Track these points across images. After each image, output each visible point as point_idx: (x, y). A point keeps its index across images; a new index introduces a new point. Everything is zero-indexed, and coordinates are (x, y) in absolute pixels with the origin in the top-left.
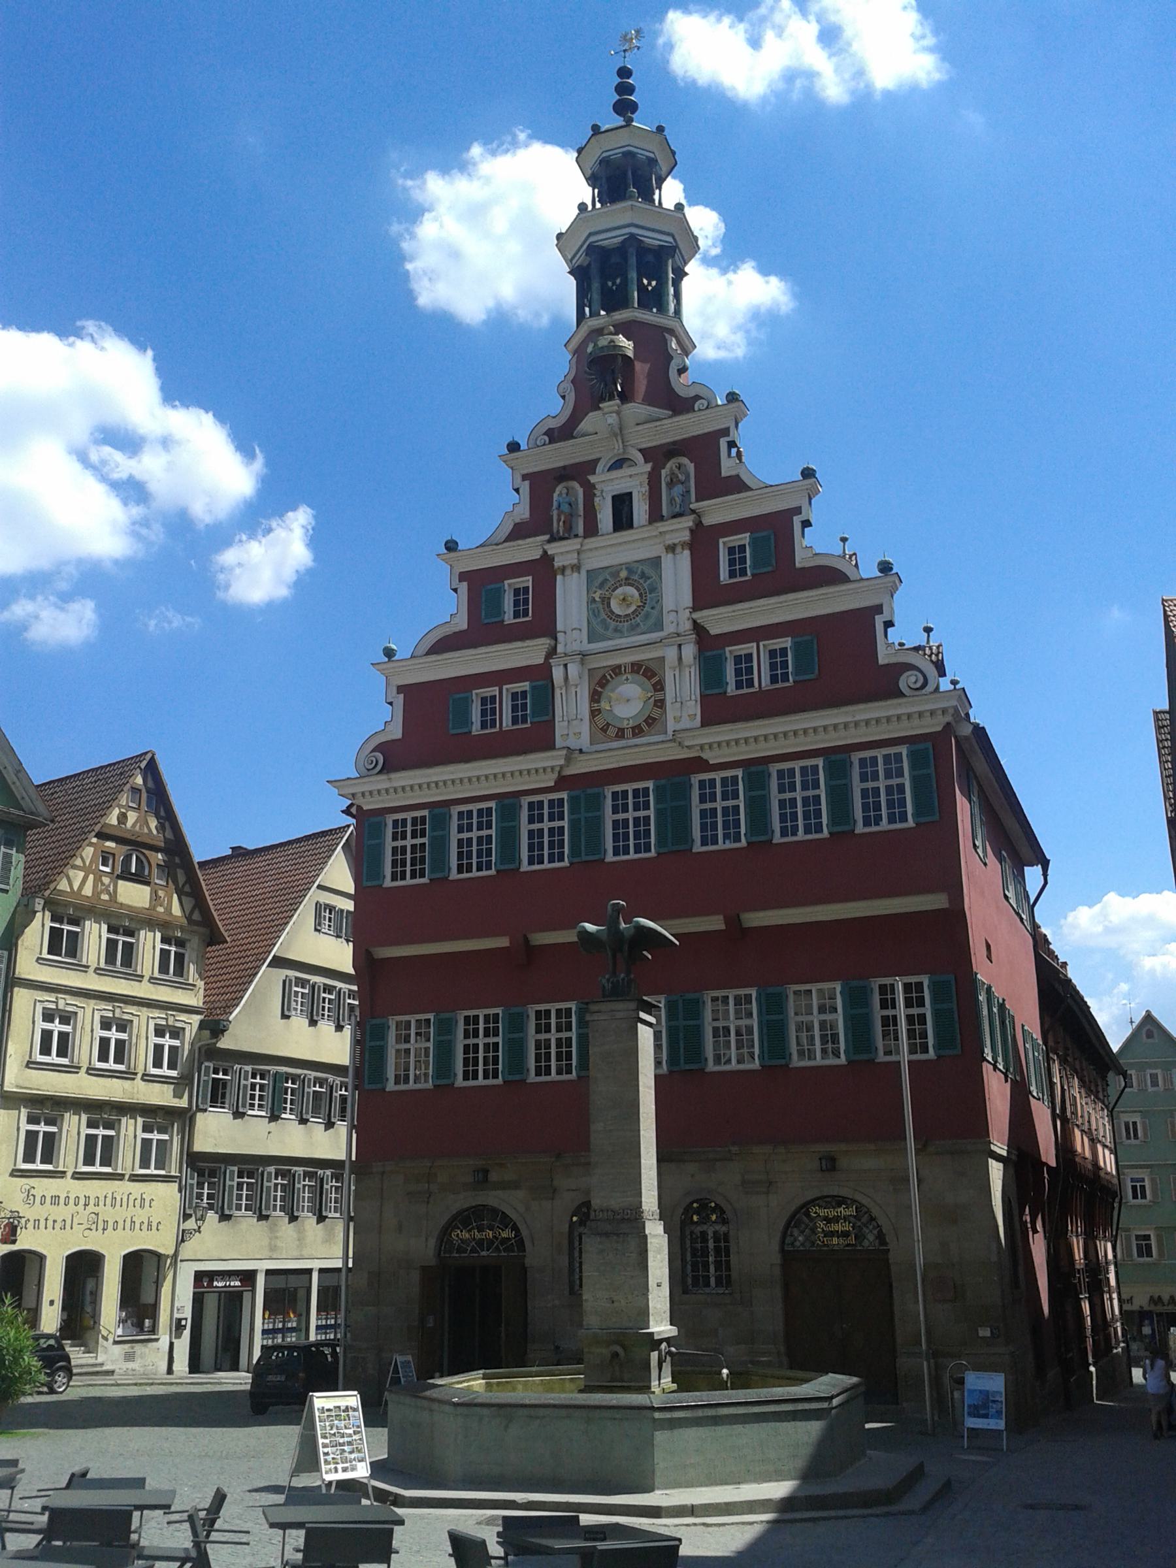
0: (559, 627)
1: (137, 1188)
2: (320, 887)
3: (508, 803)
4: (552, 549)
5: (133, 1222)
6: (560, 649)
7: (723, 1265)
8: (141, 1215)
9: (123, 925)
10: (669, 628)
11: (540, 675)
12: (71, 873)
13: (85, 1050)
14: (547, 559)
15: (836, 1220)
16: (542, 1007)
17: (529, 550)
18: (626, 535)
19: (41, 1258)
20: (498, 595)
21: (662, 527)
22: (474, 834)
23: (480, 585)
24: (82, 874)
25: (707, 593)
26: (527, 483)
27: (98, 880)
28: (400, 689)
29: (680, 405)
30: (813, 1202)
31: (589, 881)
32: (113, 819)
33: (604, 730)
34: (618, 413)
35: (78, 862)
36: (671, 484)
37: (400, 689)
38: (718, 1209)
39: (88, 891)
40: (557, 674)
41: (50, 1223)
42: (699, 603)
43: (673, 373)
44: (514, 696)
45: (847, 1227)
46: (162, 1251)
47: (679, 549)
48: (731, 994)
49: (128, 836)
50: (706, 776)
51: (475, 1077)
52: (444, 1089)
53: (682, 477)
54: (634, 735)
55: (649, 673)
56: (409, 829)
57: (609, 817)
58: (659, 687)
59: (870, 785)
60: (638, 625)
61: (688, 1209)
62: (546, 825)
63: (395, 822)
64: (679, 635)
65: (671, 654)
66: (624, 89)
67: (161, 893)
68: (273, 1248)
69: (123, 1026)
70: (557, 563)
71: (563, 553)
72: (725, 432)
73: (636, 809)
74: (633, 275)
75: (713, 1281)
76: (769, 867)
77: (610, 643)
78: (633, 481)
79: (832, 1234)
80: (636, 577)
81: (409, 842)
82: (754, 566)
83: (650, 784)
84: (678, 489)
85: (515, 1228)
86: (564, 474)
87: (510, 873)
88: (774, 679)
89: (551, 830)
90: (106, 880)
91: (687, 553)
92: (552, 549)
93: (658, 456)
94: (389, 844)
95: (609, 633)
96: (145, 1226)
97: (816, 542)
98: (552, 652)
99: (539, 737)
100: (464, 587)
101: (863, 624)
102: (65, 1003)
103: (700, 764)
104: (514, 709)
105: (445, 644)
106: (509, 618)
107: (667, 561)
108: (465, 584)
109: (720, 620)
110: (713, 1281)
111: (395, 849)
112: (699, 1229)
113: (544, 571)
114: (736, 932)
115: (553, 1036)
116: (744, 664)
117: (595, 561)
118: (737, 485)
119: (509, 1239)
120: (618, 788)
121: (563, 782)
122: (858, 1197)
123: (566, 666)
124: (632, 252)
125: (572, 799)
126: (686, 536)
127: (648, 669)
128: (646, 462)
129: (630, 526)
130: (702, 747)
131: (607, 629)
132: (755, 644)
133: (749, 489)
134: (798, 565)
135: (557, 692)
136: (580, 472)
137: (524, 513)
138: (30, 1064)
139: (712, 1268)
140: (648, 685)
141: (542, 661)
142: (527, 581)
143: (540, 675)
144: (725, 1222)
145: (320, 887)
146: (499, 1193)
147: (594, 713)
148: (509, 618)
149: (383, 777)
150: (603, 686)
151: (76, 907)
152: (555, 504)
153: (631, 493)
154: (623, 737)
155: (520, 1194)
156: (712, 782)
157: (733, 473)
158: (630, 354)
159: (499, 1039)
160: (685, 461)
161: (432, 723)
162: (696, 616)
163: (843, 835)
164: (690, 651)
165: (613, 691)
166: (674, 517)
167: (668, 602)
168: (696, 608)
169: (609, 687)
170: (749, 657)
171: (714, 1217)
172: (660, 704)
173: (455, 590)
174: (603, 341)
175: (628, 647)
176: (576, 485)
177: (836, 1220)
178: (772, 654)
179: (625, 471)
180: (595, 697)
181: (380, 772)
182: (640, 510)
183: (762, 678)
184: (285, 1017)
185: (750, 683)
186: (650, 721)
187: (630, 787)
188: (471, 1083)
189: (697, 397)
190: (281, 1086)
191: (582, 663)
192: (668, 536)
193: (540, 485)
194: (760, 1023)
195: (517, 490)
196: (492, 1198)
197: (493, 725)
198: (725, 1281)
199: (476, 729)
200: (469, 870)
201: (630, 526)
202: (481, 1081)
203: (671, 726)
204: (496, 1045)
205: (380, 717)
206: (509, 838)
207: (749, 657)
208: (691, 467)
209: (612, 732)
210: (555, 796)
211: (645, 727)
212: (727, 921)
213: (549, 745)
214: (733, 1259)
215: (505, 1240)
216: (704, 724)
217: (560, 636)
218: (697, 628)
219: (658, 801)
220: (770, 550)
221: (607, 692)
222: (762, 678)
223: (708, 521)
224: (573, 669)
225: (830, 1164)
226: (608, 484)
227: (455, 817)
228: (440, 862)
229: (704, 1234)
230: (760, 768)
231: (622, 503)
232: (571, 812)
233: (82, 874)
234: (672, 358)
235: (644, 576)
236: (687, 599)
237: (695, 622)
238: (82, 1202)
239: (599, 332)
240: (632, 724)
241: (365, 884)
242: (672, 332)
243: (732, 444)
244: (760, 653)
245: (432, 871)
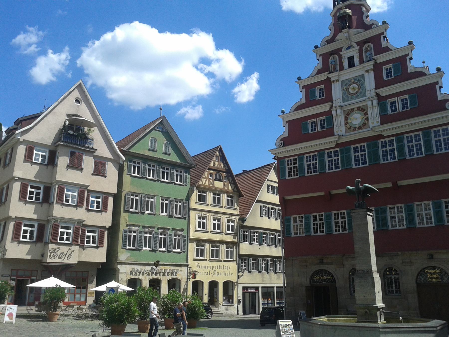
0: (333, 99)
1: (225, 264)
2: (268, 180)
3: (321, 153)
4: (330, 76)
5: (225, 273)
6: (334, 105)
7: (398, 287)
8: (227, 271)
9: (217, 193)
10: (368, 95)
11: (329, 114)
12: (202, 179)
13: (209, 227)
14: (328, 79)
15: (434, 273)
16: (336, 212)
17: (323, 77)
18: (353, 69)
19: (202, 282)
20: (314, 92)
21: (364, 65)
22: (311, 162)
23: (308, 89)
24: (205, 180)
25: (379, 83)
26: (321, 57)
27: (209, 181)
28: (287, 122)
29: (367, 27)
30: (426, 268)
31: (348, 175)
32: (212, 164)
33: (350, 128)
34: (348, 32)
35: (204, 176)
36: (366, 52)
37: (287, 122)
38: (395, 270)
39: (207, 184)
40: (334, 113)
41: (204, 273)
42: (378, 87)
44: (321, 121)
45: (438, 276)
46: (233, 281)
47: (370, 71)
48: (396, 206)
49: (216, 169)
50: (383, 140)
52: (308, 236)
53: (369, 49)
54: (359, 129)
55: (363, 110)
56: (292, 162)
57: (353, 155)
58: (366, 114)
59: (438, 139)
60: (358, 96)
61: (386, 271)
62: (333, 158)
63: (288, 160)
64: (371, 97)
65: (369, 103)
67: (226, 184)
68: (263, 281)
69: (219, 220)
70: (332, 80)
72: (382, 33)
73: (361, 152)
75: (394, 292)
76: (406, 167)
77: (350, 102)
78: (354, 52)
79: (433, 278)
80: (357, 81)
81: (292, 166)
82: (395, 74)
83: (365, 144)
84: (369, 53)
85: (332, 276)
86: (332, 53)
87: (323, 173)
88: (403, 108)
89: (335, 160)
90: (211, 181)
91: (372, 72)
92: (330, 76)
93: (361, 44)
94: (287, 167)
95: (349, 99)
96: (228, 274)
97: (415, 64)
98: (332, 107)
99: (330, 132)
100: (304, 90)
101: (432, 88)
102: (203, 214)
103: (381, 136)
104: (321, 125)
105: (299, 108)
106: (318, 98)
107: (366, 75)
108: (304, 90)
109: (384, 92)
110: (394, 292)
111: (288, 168)
112: (389, 276)
113: (328, 83)
114: (396, 187)
115: (340, 220)
116: (393, 104)
117: (343, 78)
118: (387, 49)
119: (331, 279)
120: (355, 146)
121: (338, 145)
122: (441, 267)
123: (336, 110)
125: (341, 150)
126: (372, 67)
127: (362, 109)
128: (358, 46)
129: (354, 66)
130: (381, 131)
131: (348, 97)
132: (396, 98)
133: (391, 50)
134: (409, 72)
135: (334, 118)
136: (337, 52)
137: (320, 66)
138: (196, 231)
139: (394, 288)
140: (363, 114)
141: (329, 109)
142: (323, 86)
143: (329, 114)
144: (397, 274)
145: (268, 180)
146: (327, 266)
147: (346, 124)
148: (318, 98)
149: (284, 148)
150: (348, 115)
151: (204, 188)
152: (330, 62)
153: (353, 56)
154: (356, 130)
156: (385, 141)
157: (386, 46)
158: (351, 14)
159: (324, 222)
160: (370, 44)
161: (297, 131)
162: (376, 91)
163: (430, 155)
164: (375, 102)
165: (351, 116)
166: (367, 61)
167: (367, 87)
168: (376, 88)
169: (350, 115)
170: (395, 102)
171: (394, 273)
172: (367, 119)
173: (301, 91)
174: (342, 11)
175: (356, 103)
176: (336, 56)
177: (434, 273)
178: (402, 100)
179: (351, 49)
180: (346, 119)
181: (283, 146)
182: (357, 61)
183: (400, 108)
184: (261, 216)
185: (396, 110)
186: (364, 125)
187: (359, 145)
188: (316, 234)
189: (373, 24)
190: (262, 236)
191: (341, 109)
192: (366, 68)
193: (325, 57)
194: (406, 214)
195: (318, 60)
196: (326, 267)
197: (315, 130)
198: (398, 291)
199: (310, 132)
200: (311, 173)
201: (354, 66)
202: (319, 234)
203: (371, 125)
204: (323, 223)
205: (281, 130)
206: (322, 163)
207: (395, 102)
208: (372, 46)
209: (352, 129)
211: (362, 126)
212: (393, 184)
213: (332, 134)
214: (401, 285)
216: (382, 124)
217: (334, 102)
218: (377, 95)
219: (368, 149)
220: (400, 67)
221: (350, 117)
222: (400, 108)
223: (378, 61)
224: (339, 111)
225: (431, 257)
226: (346, 54)
227: (305, 158)
228: (302, 171)
229: (391, 278)
230: (402, 136)
232: (341, 154)
233: (205, 180)
234: (364, 13)
236: (373, 86)
237: (376, 93)
238: (212, 267)
239: (341, 9)
240: (358, 126)
241: (281, 178)
242: (363, 5)
243: (385, 37)
244: (398, 101)
245: (299, 174)
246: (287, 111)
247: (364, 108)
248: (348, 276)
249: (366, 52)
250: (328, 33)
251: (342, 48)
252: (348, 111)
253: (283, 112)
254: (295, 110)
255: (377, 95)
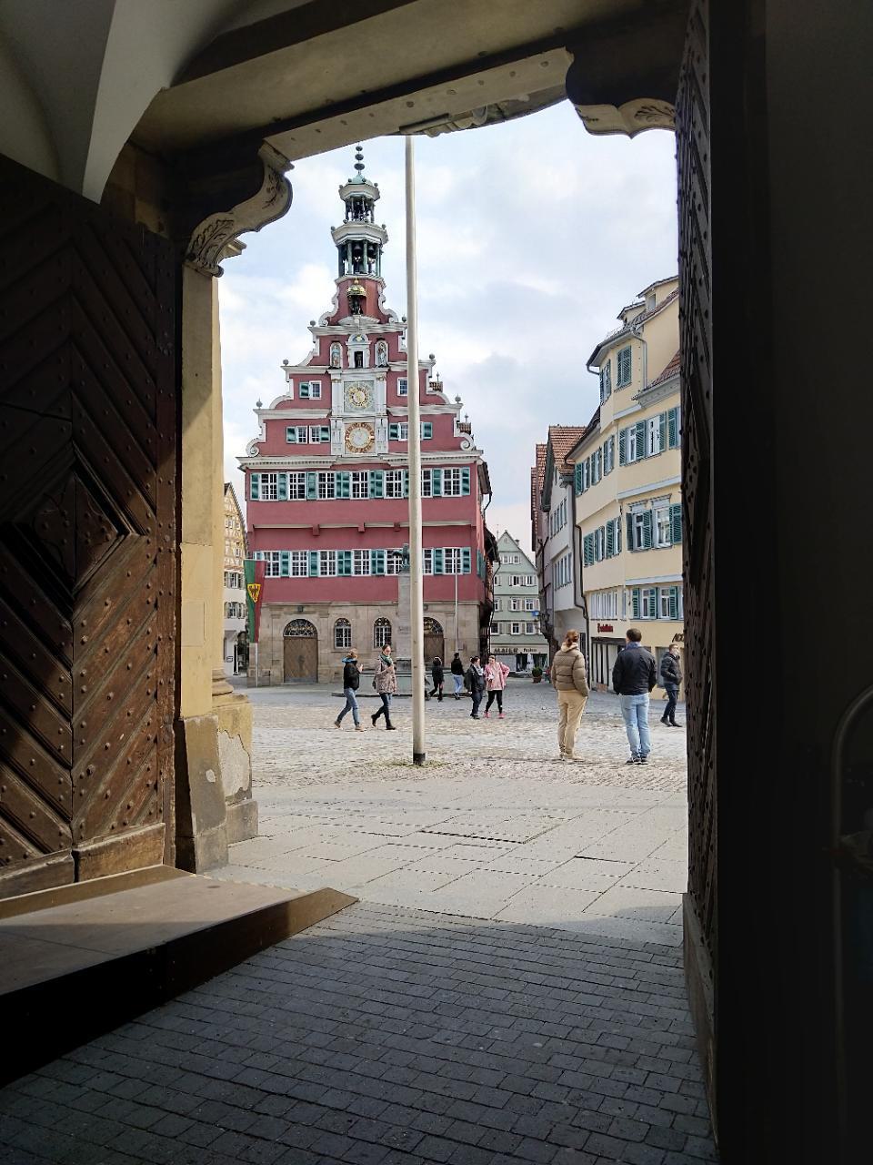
17: (320, 370)
18: (361, 371)
23: (297, 377)
29: (384, 318)
38: (388, 622)
43: (380, 300)
51: (298, 574)
58: (372, 433)
61: (377, 621)
66: (359, 157)
70: (333, 377)
71: (334, 374)
74: (365, 256)
85: (313, 626)
91: (385, 382)
98: (330, 414)
103: (386, 466)
105: (282, 405)
124: (365, 245)
155: (316, 615)
160: (385, 342)
164: (385, 421)
174: (355, 289)
180: (347, 434)
189: (390, 316)
202: (300, 576)
210: (331, 472)
215: (308, 631)
231: (358, 355)
235: (365, 388)
246: (265, 406)
247: (371, 425)
248: (332, 627)
249: (380, 351)
250: (331, 309)
251: (349, 335)
252: (348, 426)
253: (259, 404)
254: (277, 408)
255: (388, 412)
